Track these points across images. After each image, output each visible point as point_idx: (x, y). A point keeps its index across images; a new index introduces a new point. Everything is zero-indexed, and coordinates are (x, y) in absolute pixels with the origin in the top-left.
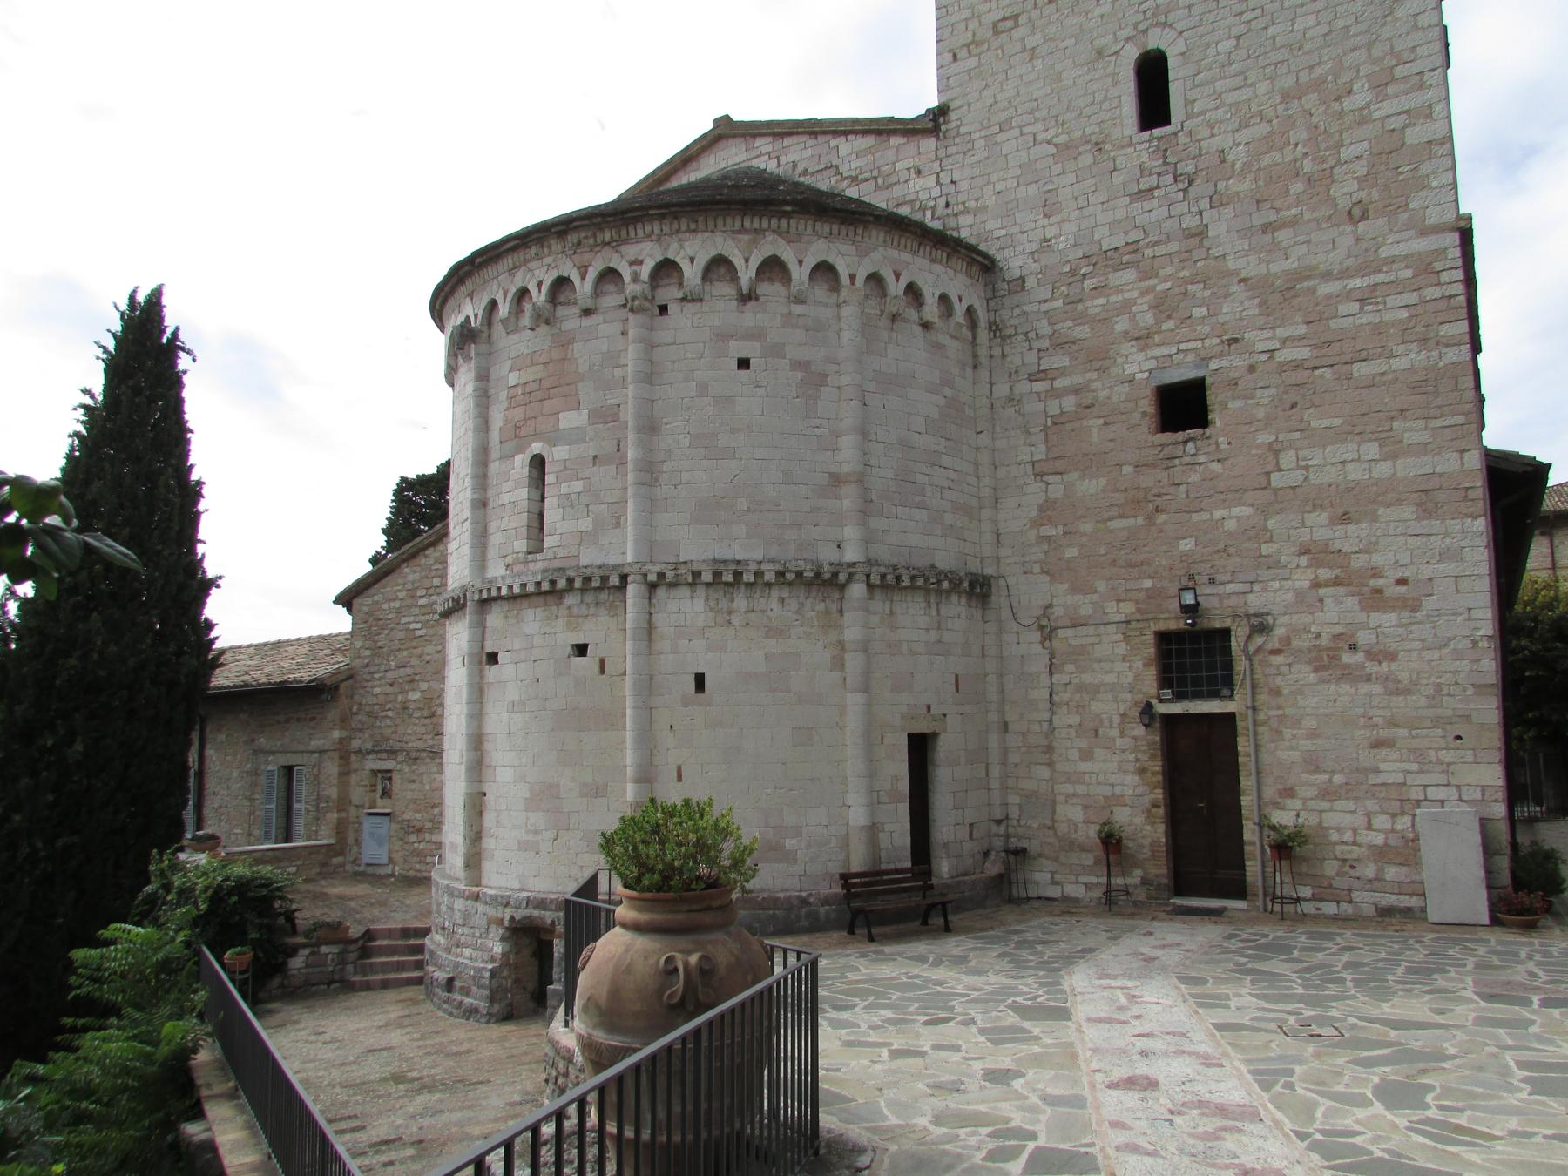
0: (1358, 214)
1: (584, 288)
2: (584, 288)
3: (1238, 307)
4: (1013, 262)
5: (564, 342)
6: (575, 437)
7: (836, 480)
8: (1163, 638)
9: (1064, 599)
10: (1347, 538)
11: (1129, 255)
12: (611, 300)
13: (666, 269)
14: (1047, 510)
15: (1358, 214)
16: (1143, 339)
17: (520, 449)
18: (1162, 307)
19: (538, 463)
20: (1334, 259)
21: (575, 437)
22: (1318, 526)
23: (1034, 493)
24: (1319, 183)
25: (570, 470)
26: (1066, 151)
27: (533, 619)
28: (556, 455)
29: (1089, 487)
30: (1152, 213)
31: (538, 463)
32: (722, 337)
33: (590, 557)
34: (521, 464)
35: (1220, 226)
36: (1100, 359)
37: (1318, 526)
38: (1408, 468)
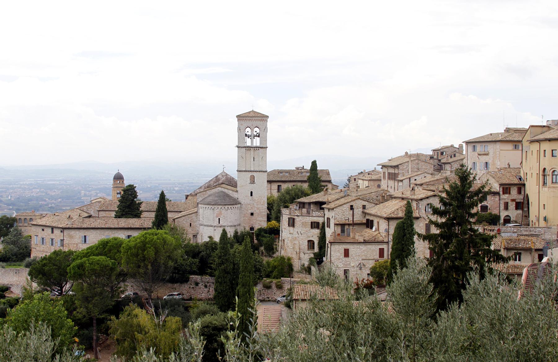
0: (262, 205)
1: (223, 208)
2: (223, 208)
3: (256, 209)
4: (242, 203)
5: (221, 211)
6: (222, 217)
7: (236, 220)
8: (250, 228)
9: (244, 225)
10: (260, 223)
11: (249, 204)
12: (224, 209)
13: (228, 207)
14: (244, 220)
15: (262, 205)
16: (250, 210)
17: (217, 217)
18: (251, 208)
19: (219, 219)
20: (261, 207)
21: (222, 217)
22: (259, 222)
23: (243, 219)
24: (260, 202)
25: (222, 219)
26: (246, 196)
27: (219, 228)
28: (221, 218)
29: (247, 218)
30: (251, 202)
31: (219, 219)
32: (231, 212)
33: (223, 225)
34: (218, 218)
35: (255, 204)
36: (247, 210)
37: (259, 222)
38: (264, 219)
